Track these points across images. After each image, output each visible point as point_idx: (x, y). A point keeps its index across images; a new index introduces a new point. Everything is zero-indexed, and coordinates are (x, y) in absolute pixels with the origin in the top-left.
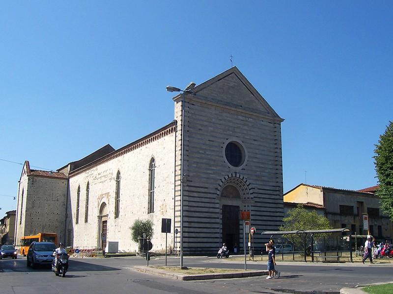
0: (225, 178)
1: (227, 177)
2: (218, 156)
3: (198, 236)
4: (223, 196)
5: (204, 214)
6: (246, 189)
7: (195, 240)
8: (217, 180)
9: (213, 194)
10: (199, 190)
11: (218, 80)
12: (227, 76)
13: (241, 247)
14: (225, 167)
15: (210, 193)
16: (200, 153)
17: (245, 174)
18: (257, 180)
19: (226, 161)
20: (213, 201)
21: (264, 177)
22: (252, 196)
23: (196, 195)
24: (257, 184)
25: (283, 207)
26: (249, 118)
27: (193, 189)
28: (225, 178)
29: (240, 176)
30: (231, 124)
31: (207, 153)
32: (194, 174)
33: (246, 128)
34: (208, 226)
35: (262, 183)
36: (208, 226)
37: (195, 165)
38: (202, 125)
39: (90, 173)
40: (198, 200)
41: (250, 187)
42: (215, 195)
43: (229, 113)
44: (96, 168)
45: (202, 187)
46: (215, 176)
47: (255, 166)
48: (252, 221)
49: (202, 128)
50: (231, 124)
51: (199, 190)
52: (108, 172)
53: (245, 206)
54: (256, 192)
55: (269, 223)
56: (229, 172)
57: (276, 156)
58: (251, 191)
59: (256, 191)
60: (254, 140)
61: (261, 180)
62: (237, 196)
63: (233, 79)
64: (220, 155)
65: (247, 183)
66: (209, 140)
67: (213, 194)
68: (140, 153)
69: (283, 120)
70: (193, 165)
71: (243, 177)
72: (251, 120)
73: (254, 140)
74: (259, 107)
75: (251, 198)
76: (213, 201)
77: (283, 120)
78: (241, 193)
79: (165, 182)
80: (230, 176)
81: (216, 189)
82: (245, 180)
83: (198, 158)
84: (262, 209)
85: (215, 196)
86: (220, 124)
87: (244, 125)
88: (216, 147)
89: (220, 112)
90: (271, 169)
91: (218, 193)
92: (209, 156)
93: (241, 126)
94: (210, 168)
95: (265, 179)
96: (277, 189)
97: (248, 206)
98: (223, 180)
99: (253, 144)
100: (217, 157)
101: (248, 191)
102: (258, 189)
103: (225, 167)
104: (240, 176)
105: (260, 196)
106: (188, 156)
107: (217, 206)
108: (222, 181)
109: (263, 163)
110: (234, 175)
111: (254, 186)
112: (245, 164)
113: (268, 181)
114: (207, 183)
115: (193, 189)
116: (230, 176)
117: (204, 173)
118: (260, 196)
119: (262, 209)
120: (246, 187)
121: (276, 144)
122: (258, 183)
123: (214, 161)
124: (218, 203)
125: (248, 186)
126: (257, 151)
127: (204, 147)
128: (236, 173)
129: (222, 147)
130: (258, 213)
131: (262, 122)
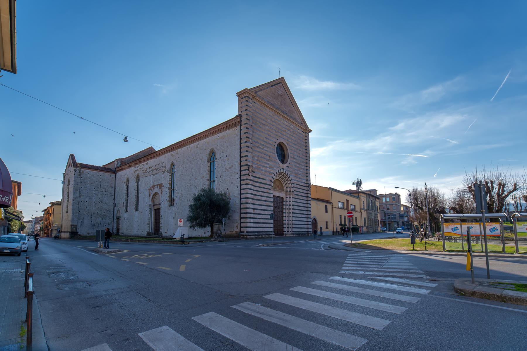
0: (276, 172)
1: (278, 172)
2: (272, 153)
3: (260, 222)
4: (275, 189)
6: (288, 184)
7: (257, 225)
8: (271, 173)
9: (269, 185)
13: (284, 232)
15: (267, 184)
16: (260, 148)
18: (296, 177)
20: (269, 191)
22: (293, 189)
23: (257, 184)
24: (295, 180)
27: (255, 179)
28: (276, 172)
30: (280, 127)
32: (256, 166)
33: (289, 132)
35: (298, 180)
37: (257, 158)
39: (139, 167)
41: (292, 181)
42: (271, 186)
44: (146, 162)
45: (261, 179)
46: (270, 169)
48: (293, 210)
49: (261, 126)
52: (160, 166)
53: (288, 198)
54: (295, 186)
55: (302, 212)
56: (279, 167)
58: (293, 185)
59: (296, 186)
60: (294, 144)
62: (282, 189)
64: (273, 152)
65: (290, 179)
67: (269, 185)
68: (196, 148)
69: (310, 131)
71: (288, 174)
72: (292, 127)
73: (294, 144)
75: (292, 191)
76: (269, 191)
77: (310, 131)
78: (285, 186)
79: (227, 172)
80: (280, 171)
81: (271, 181)
82: (288, 176)
83: (259, 152)
84: (299, 201)
85: (269, 187)
86: (273, 125)
87: (288, 130)
90: (303, 169)
91: (272, 184)
92: (266, 152)
93: (286, 130)
94: (267, 162)
95: (300, 176)
96: (308, 186)
97: (290, 198)
98: (275, 174)
99: (294, 147)
100: (271, 154)
106: (252, 148)
107: (272, 196)
108: (274, 175)
109: (299, 164)
112: (288, 162)
115: (255, 179)
116: (280, 171)
119: (299, 201)
121: (306, 149)
122: (296, 179)
124: (272, 194)
125: (290, 181)
127: (262, 143)
128: (283, 169)
130: (296, 204)
131: (298, 130)
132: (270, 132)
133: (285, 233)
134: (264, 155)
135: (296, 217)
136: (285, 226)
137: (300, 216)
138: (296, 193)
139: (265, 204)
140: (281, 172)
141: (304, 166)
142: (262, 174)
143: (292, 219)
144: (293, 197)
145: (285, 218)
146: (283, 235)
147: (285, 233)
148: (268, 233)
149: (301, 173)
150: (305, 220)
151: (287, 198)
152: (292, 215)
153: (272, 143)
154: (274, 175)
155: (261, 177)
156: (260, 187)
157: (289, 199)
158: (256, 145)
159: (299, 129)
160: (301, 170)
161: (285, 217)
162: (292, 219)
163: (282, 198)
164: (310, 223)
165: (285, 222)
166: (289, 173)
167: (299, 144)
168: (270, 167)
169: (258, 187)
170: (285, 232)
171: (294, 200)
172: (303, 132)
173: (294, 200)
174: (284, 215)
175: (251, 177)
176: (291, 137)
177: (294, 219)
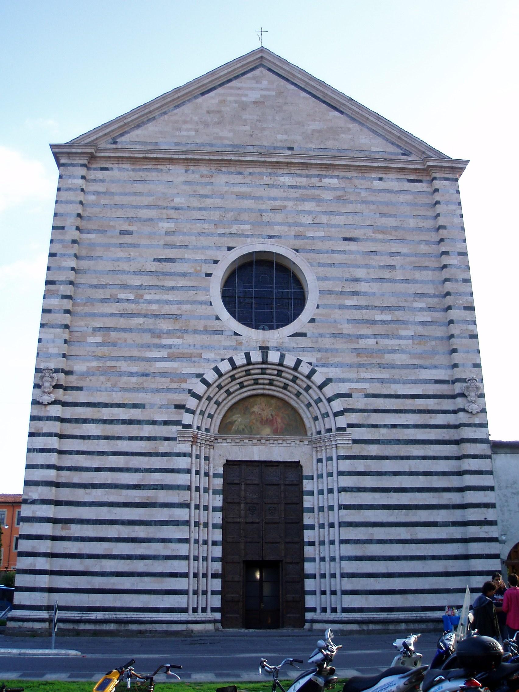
0: (216, 370)
1: (225, 367)
5: (125, 492)
8: (183, 378)
9: (166, 423)
10: (106, 413)
11: (203, 94)
12: (236, 77)
14: (220, 333)
15: (154, 423)
17: (304, 350)
18: (360, 366)
19: (225, 315)
20: (164, 447)
21: (393, 351)
22: (342, 421)
24: (359, 380)
25: (489, 452)
26: (320, 177)
28: (216, 370)
29: (282, 357)
31: (147, 297)
33: (309, 206)
34: (140, 532)
36: (140, 532)
37: (99, 339)
38: (131, 220)
40: (103, 445)
41: (329, 391)
42: (175, 428)
43: (240, 173)
47: (349, 321)
48: (343, 512)
50: (248, 204)
51: (106, 413)
57: (446, 280)
58: (337, 405)
59: (360, 402)
60: (345, 239)
61: (380, 366)
63: (257, 82)
65: (318, 379)
66: (159, 260)
67: (166, 423)
70: (90, 339)
73: (345, 239)
74: (363, 141)
76: (164, 447)
82: (305, 369)
85: (173, 431)
86: (200, 209)
87: (303, 199)
88: (184, 275)
89: (202, 176)
92: (155, 307)
93: (290, 204)
94: (157, 341)
96: (457, 391)
100: (188, 307)
101: (324, 407)
102: (367, 396)
103: (220, 333)
104: (282, 357)
105: (376, 419)
108: (204, 381)
110: (256, 357)
111: (343, 388)
113: (415, 367)
114: (145, 390)
117: (126, 359)
118: (376, 419)
120: (314, 393)
121: (442, 240)
123: (176, 317)
125: (321, 387)
126: (360, 273)
127: (136, 281)
129: (209, 275)
132: (185, 234)
133: (309, 616)
134: (141, 320)
135: (369, 542)
136: (309, 585)
137: (403, 533)
138: (357, 433)
139: (137, 500)
140: (249, 363)
141: (430, 309)
142: (124, 390)
143: (337, 550)
144: (342, 453)
145: (308, 551)
147: (309, 616)
149: (410, 342)
151: (320, 461)
152: (335, 534)
154: (204, 381)
155: (117, 401)
156: (107, 438)
157: (323, 468)
158: (100, 294)
159: (381, 179)
160: (403, 333)
161: (312, 544)
162: (337, 550)
163: (296, 466)
165: (309, 568)
166: (306, 358)
167: (382, 232)
168: (171, 358)
169: (98, 438)
170: (314, 610)
171: (345, 465)
172: (420, 181)
173: (345, 465)
174: (308, 535)
175: (50, 408)
176: (324, 219)
177: (349, 550)
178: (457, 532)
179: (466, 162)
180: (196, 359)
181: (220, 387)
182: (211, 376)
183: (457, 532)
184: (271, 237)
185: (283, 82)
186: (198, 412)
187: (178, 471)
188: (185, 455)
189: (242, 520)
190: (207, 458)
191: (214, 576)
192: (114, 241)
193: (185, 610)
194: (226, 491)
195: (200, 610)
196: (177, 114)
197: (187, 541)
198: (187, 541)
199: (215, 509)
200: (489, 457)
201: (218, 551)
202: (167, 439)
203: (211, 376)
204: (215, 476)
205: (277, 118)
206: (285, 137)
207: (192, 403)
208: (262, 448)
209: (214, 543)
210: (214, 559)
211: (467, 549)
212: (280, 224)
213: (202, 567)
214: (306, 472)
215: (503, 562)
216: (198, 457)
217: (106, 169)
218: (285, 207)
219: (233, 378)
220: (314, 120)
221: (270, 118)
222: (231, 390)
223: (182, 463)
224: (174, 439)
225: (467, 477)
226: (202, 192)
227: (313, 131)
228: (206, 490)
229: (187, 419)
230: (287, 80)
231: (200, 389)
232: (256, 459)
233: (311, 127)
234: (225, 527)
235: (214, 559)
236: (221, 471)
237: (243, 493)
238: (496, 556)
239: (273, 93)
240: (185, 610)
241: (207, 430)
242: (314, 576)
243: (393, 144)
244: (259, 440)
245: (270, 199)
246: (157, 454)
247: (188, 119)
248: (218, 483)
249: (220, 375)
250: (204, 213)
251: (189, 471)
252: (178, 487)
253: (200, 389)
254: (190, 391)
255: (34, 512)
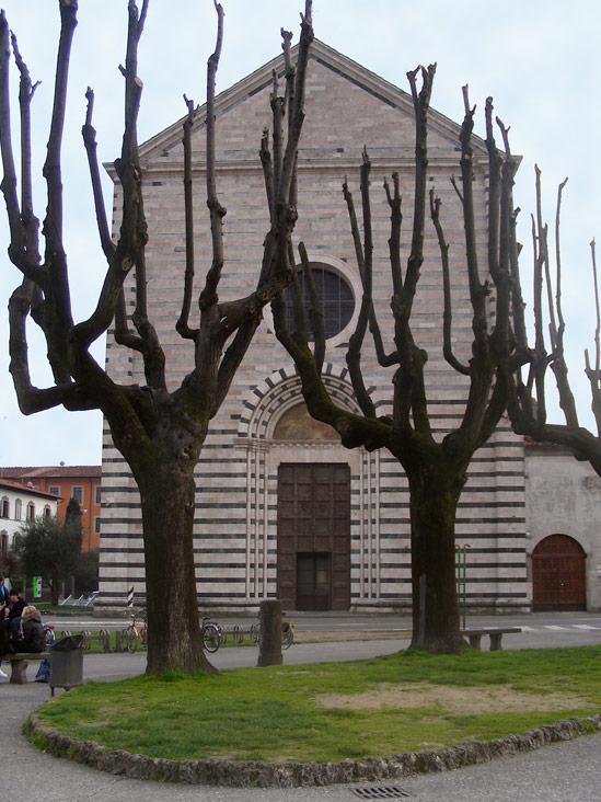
0: (268, 381)
1: (276, 378)
9: (223, 432)
11: (251, 94)
28: (268, 381)
42: (231, 436)
85: (230, 439)
86: (251, 221)
89: (252, 186)
108: (257, 393)
133: (353, 600)
146: (348, 608)
147: (353, 600)
148: (215, 600)
150: (503, 543)
151: (365, 462)
152: (376, 530)
153: (244, 285)
154: (257, 393)
161: (358, 537)
163: (345, 467)
164: (521, 558)
165: (355, 558)
170: (358, 595)
174: (354, 530)
178: (488, 528)
179: (522, 157)
180: (250, 372)
181: (272, 397)
182: (263, 388)
183: (488, 528)
184: (319, 247)
185: (333, 75)
186: (253, 420)
187: (236, 475)
188: (241, 461)
189: (295, 517)
190: (262, 462)
191: (270, 566)
192: (170, 258)
193: (244, 595)
194: (280, 491)
195: (257, 595)
196: (225, 119)
197: (244, 536)
198: (244, 536)
199: (270, 507)
200: (522, 459)
201: (273, 545)
202: (225, 447)
203: (263, 388)
204: (270, 477)
205: (327, 116)
206: (335, 138)
207: (247, 413)
208: (313, 451)
209: (270, 537)
210: (269, 552)
211: (497, 544)
212: (329, 233)
213: (258, 558)
214: (353, 473)
215: (528, 556)
216: (253, 461)
217: (159, 184)
218: (334, 215)
219: (284, 388)
220: (365, 117)
221: (320, 117)
222: (284, 398)
223: (239, 468)
224: (231, 447)
225: (499, 478)
226: (252, 204)
227: (364, 128)
228: (262, 491)
229: (242, 427)
230: (338, 71)
231: (254, 400)
232: (308, 461)
233: (363, 125)
234: (280, 522)
235: (269, 552)
236: (275, 473)
237: (296, 493)
238: (522, 550)
239: (323, 88)
240: (244, 595)
241: (262, 436)
242: (358, 566)
243: (446, 138)
244: (310, 444)
245: (319, 207)
246: (216, 461)
247: (237, 124)
248: (274, 483)
249: (272, 386)
250: (255, 225)
251: (245, 475)
252: (236, 490)
253: (254, 400)
254: (244, 402)
255: (112, 514)
